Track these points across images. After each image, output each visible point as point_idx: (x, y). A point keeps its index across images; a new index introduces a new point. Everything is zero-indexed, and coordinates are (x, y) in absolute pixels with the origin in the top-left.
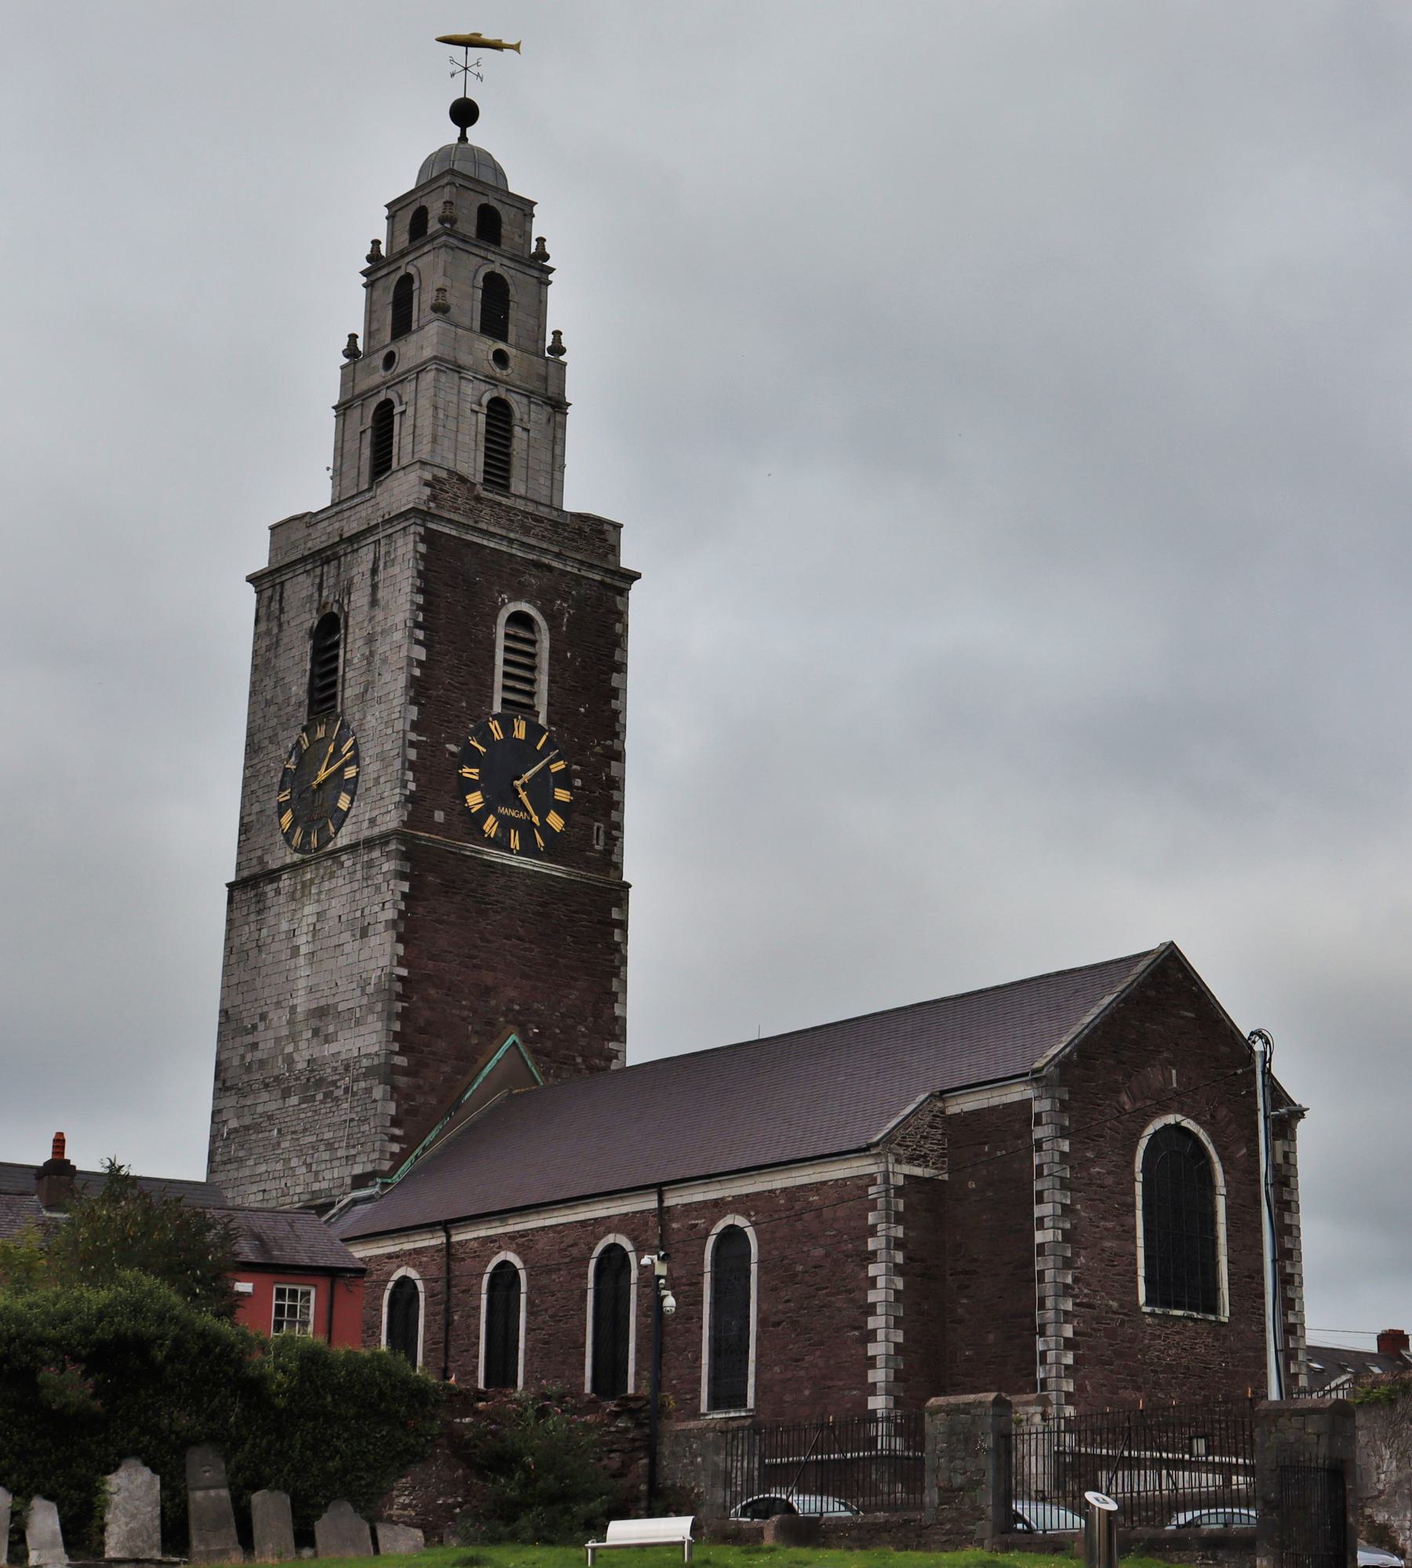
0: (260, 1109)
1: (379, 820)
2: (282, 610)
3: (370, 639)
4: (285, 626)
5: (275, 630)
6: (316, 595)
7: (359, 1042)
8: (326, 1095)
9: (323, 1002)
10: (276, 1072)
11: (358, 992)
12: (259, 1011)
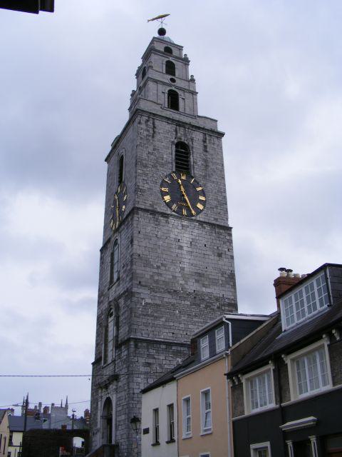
0: (166, 300)
1: (219, 220)
2: (154, 127)
3: (206, 161)
5: (151, 132)
8: (207, 307)
9: (199, 271)
11: (220, 275)
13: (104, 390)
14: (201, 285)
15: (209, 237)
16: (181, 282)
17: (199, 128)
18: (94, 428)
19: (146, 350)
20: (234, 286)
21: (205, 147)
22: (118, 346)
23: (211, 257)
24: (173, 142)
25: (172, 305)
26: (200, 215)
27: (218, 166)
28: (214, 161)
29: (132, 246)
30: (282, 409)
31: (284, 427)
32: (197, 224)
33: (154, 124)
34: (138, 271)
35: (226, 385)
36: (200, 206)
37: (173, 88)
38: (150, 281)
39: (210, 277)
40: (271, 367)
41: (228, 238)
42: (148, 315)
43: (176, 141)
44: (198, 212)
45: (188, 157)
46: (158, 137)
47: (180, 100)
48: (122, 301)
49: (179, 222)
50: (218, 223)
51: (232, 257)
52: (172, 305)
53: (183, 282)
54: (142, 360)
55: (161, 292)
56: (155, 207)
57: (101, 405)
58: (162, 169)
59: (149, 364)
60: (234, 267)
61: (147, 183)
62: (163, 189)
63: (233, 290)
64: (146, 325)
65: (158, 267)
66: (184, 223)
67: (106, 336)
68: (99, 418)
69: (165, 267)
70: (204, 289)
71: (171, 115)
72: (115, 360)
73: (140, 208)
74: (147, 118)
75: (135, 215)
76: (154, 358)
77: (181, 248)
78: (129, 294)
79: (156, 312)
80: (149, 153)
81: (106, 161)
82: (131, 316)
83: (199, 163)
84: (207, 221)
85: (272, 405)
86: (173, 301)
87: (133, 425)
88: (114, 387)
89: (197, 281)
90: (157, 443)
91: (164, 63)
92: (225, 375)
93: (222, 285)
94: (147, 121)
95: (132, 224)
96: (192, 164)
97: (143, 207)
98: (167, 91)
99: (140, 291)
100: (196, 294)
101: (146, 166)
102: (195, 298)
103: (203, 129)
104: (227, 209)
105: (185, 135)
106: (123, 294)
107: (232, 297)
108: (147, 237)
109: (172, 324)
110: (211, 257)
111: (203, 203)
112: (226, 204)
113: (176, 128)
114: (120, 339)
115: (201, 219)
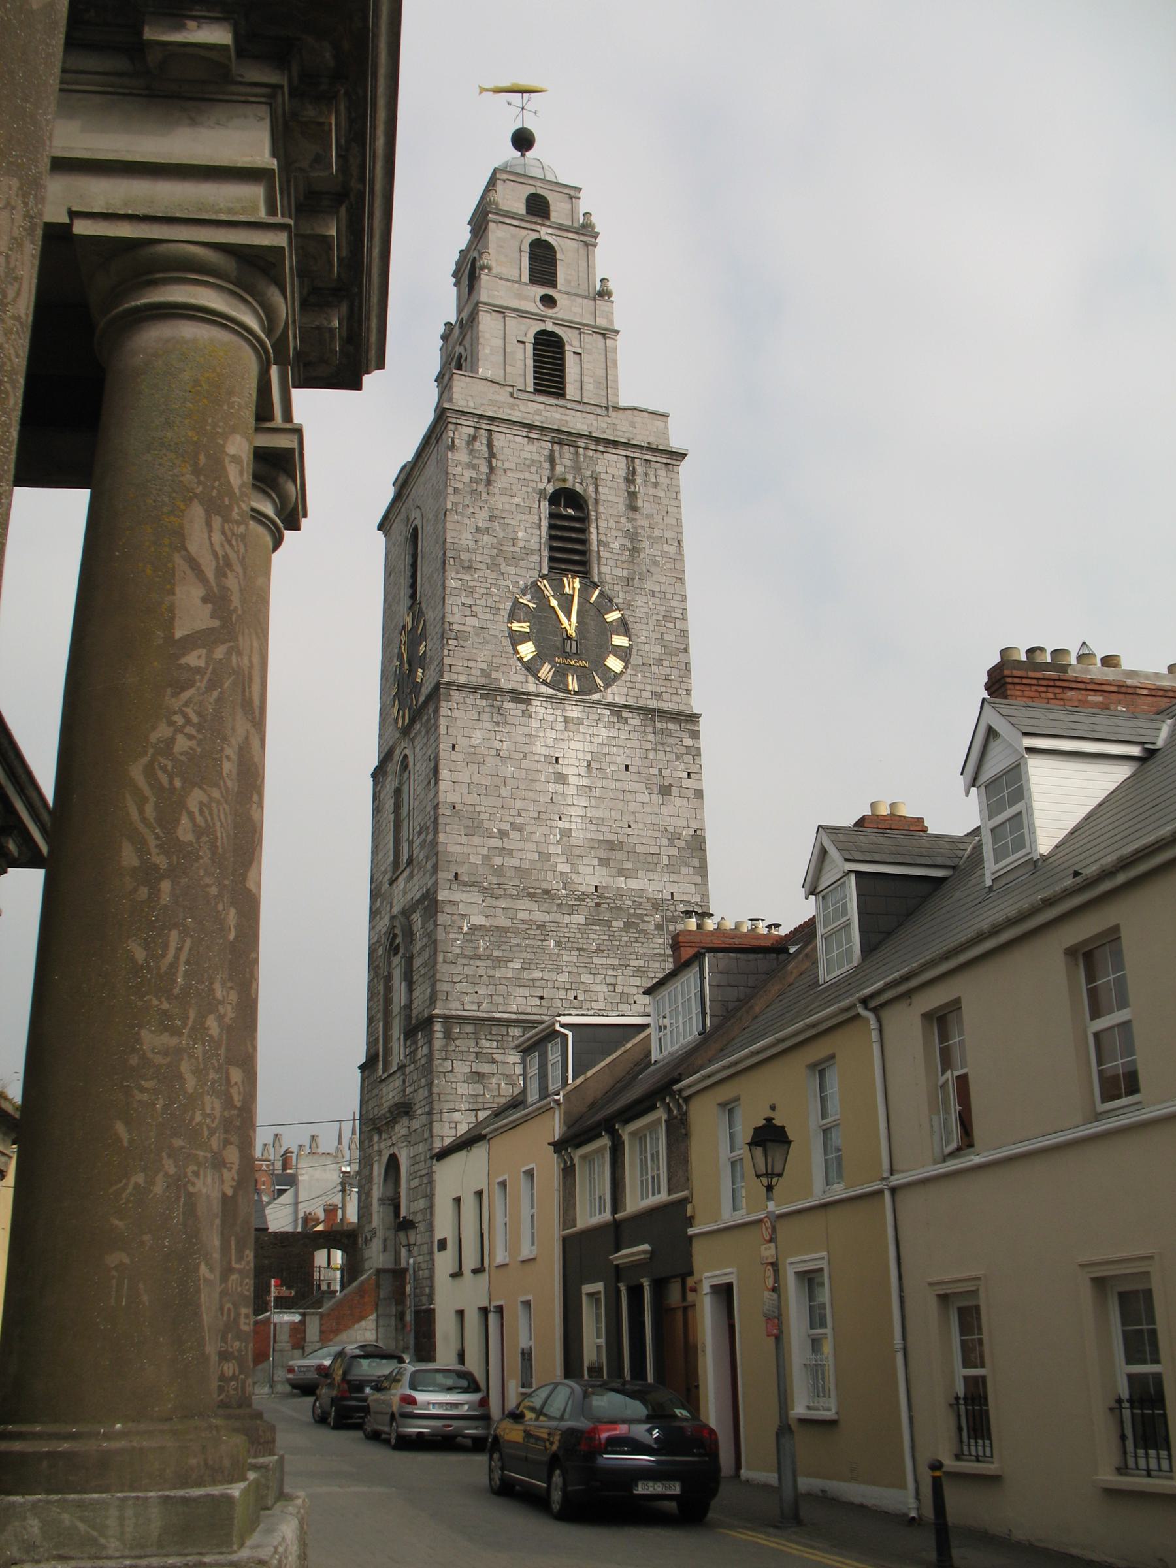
0: (522, 915)
2: (492, 455)
3: (632, 536)
5: (484, 469)
6: (547, 465)
8: (628, 926)
10: (544, 886)
11: (664, 842)
13: (384, 1136)
14: (615, 872)
15: (637, 744)
16: (560, 867)
17: (615, 444)
18: (367, 1229)
19: (472, 1043)
20: (702, 870)
21: (632, 496)
22: (410, 1033)
23: (640, 797)
24: (542, 492)
25: (539, 927)
27: (666, 548)
28: (657, 533)
29: (437, 782)
30: (617, 1225)
31: (617, 1258)
32: (607, 712)
33: (490, 445)
34: (450, 849)
35: (549, 1165)
36: (614, 664)
37: (550, 327)
38: (481, 871)
40: (605, 1141)
41: (688, 742)
42: (479, 957)
43: (550, 489)
44: (611, 678)
45: (584, 531)
46: (500, 482)
47: (570, 361)
48: (417, 918)
49: (559, 712)
50: (662, 705)
51: (699, 794)
52: (539, 927)
53: (567, 868)
54: (462, 1068)
55: (511, 896)
57: (378, 1171)
58: (512, 570)
59: (479, 1077)
60: (702, 820)
62: (515, 626)
63: (699, 880)
64: (473, 981)
65: (503, 834)
66: (569, 714)
67: (388, 1001)
68: (375, 1202)
69: (521, 830)
70: (621, 882)
71: (538, 412)
72: (405, 1066)
73: (453, 684)
74: (471, 431)
75: (443, 704)
76: (494, 1062)
77: (562, 778)
78: (429, 904)
80: (478, 529)
81: (380, 528)
82: (435, 963)
83: (615, 545)
84: (631, 702)
85: (607, 1216)
87: (402, 1235)
88: (404, 1131)
89: (603, 862)
90: (457, 1275)
91: (526, 247)
92: (550, 1144)
93: (669, 869)
94: (474, 438)
95: (437, 727)
96: (594, 547)
97: (462, 679)
98: (530, 338)
99: (456, 897)
100: (602, 897)
101: (470, 568)
102: (598, 905)
103: (627, 445)
105: (577, 469)
107: (698, 899)
108: (474, 758)
110: (640, 797)
111: (624, 654)
112: (686, 650)
113: (552, 451)
114: (414, 1013)
115: (619, 700)
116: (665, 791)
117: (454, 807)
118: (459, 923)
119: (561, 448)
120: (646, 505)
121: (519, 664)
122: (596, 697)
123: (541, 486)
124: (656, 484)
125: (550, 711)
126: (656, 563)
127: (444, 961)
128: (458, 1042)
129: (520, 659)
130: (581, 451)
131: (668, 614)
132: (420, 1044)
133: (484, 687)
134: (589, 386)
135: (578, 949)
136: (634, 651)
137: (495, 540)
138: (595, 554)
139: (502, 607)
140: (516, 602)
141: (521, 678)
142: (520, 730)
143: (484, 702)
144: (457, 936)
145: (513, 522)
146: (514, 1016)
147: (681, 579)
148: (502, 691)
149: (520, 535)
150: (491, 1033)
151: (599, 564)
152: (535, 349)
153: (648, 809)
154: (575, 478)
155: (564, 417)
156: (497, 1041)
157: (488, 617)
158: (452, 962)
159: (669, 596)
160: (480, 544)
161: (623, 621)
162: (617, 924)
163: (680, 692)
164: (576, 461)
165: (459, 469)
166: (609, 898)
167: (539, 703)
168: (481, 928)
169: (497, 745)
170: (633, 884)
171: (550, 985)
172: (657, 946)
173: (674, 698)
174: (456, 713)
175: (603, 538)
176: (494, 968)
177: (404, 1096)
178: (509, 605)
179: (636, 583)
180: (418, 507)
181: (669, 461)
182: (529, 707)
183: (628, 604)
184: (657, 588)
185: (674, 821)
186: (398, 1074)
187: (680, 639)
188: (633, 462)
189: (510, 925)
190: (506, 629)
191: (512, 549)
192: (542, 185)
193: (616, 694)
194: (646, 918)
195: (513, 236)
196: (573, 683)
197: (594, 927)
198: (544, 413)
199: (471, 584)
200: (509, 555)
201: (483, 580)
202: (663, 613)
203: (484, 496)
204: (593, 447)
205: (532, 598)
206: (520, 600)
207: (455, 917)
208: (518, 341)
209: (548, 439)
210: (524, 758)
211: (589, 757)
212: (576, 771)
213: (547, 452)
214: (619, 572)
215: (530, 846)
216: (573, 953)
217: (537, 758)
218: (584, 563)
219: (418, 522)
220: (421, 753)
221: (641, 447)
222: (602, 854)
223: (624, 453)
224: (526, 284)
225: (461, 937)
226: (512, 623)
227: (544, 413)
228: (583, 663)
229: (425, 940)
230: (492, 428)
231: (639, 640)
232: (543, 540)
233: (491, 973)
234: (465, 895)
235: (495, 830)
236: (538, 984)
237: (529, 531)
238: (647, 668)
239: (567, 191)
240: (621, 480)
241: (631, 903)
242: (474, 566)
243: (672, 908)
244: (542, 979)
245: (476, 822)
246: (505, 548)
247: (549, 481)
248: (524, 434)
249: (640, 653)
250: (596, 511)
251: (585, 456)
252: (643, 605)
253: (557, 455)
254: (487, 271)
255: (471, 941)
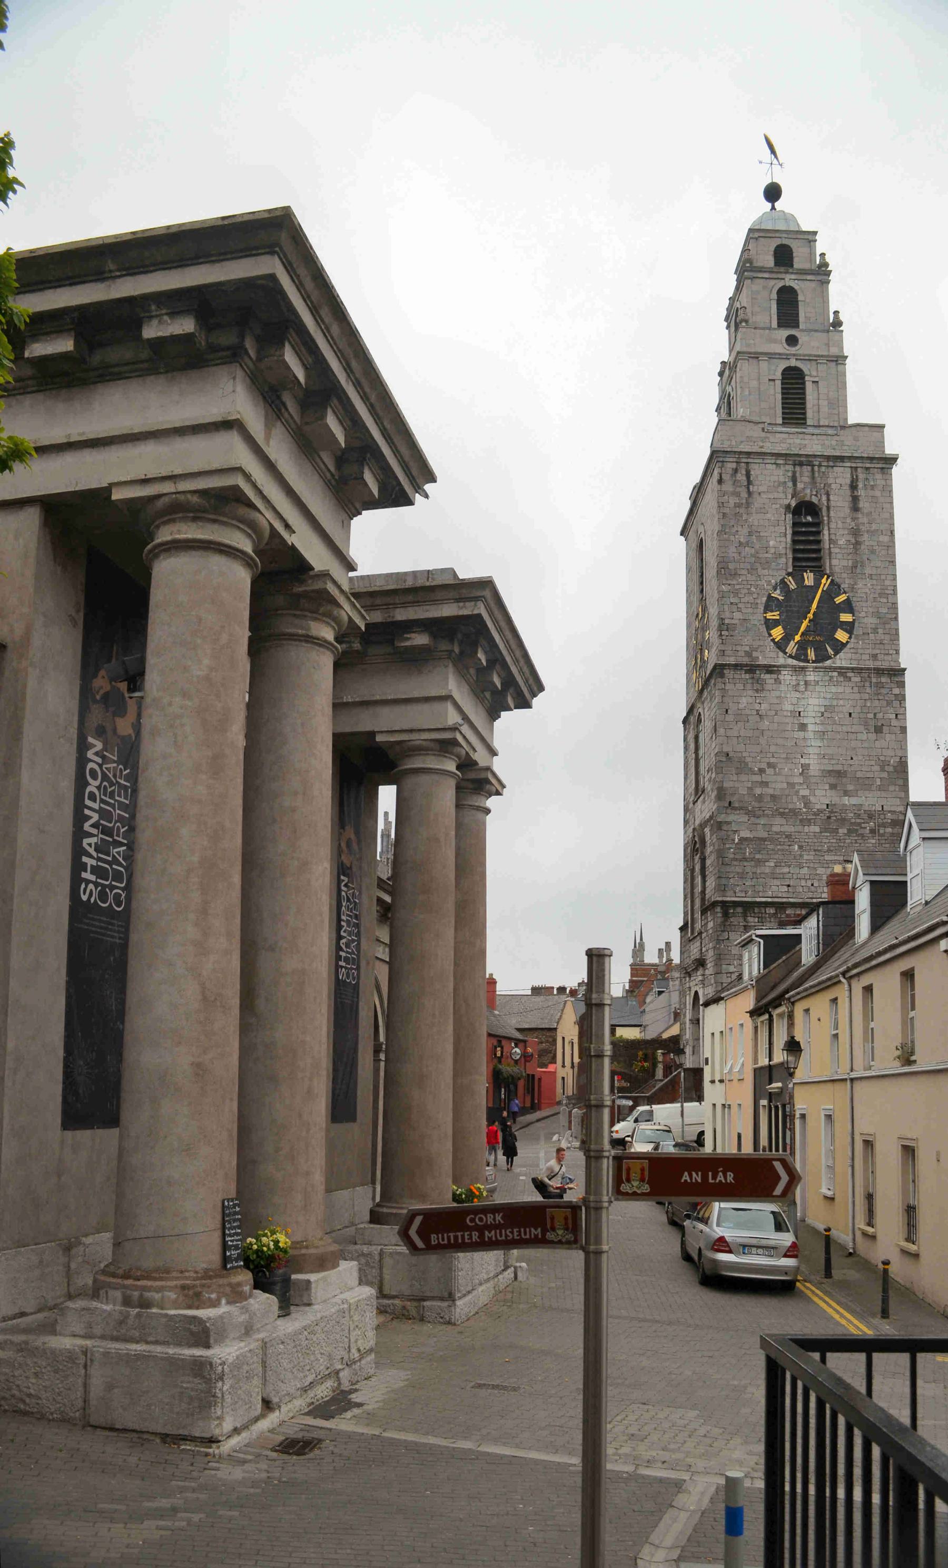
0: (775, 829)
1: (879, 657)
2: (749, 482)
3: (856, 532)
4: (755, 496)
5: (744, 495)
6: (790, 484)
7: (884, 802)
9: (839, 768)
10: (791, 806)
11: (877, 768)
12: (767, 760)
14: (842, 792)
15: (857, 696)
16: (802, 793)
17: (842, 459)
19: (741, 920)
21: (855, 499)
24: (788, 507)
25: (787, 837)
26: (841, 655)
27: (881, 538)
28: (874, 527)
32: (835, 674)
33: (748, 475)
36: (841, 636)
39: (859, 775)
41: (896, 691)
42: (745, 859)
43: (793, 504)
45: (818, 533)
46: (757, 502)
47: (809, 387)
49: (801, 678)
50: (878, 664)
51: (904, 730)
52: (787, 837)
53: (805, 792)
55: (767, 816)
56: (755, 654)
60: (906, 750)
61: (739, 610)
62: (769, 615)
63: (902, 795)
64: (742, 876)
65: (761, 771)
66: (808, 678)
70: (846, 800)
73: (726, 665)
74: (734, 466)
77: (803, 727)
79: (759, 852)
80: (740, 543)
83: (842, 542)
86: (789, 829)
89: (833, 787)
93: (880, 788)
94: (736, 471)
96: (826, 545)
97: (732, 660)
98: (778, 375)
99: (731, 818)
102: (829, 818)
104: (897, 630)
106: (709, 820)
109: (786, 870)
110: (860, 736)
111: (849, 628)
112: (896, 619)
113: (794, 473)
114: (707, 897)
115: (844, 664)
116: (878, 730)
117: (728, 755)
118: (732, 837)
119: (801, 468)
120: (867, 505)
121: (772, 644)
122: (828, 663)
123: (786, 502)
124: (873, 488)
125: (794, 678)
126: (873, 552)
127: (723, 864)
128: (732, 920)
129: (773, 640)
130: (816, 468)
131: (883, 591)
132: (709, 920)
133: (747, 665)
134: (825, 409)
135: (815, 850)
136: (856, 625)
137: (753, 551)
138: (827, 551)
139: (759, 602)
140: (769, 597)
141: (773, 655)
142: (775, 694)
143: (747, 676)
144: (731, 846)
145: (765, 534)
146: (769, 900)
147: (892, 562)
148: (759, 666)
149: (772, 543)
150: (754, 912)
151: (830, 559)
152: (782, 384)
153: (866, 745)
154: (811, 490)
155: (803, 442)
156: (758, 918)
157: (750, 610)
158: (727, 864)
159: (883, 577)
160: (743, 555)
161: (848, 602)
162: (843, 831)
163: (891, 652)
164: (813, 477)
165: (726, 497)
166: (836, 812)
167: (786, 673)
168: (746, 839)
169: (757, 707)
170: (854, 801)
171: (795, 876)
172: (871, 845)
173: (886, 658)
174: (728, 687)
175: (833, 537)
176: (756, 866)
177: (701, 953)
178: (765, 599)
179: (858, 571)
180: (702, 524)
181: (884, 466)
182: (780, 676)
183: (852, 588)
184: (874, 572)
185: (885, 752)
186: (698, 938)
187: (891, 611)
188: (856, 471)
189: (767, 836)
190: (762, 618)
191: (767, 555)
192: (786, 236)
193: (842, 660)
194: (863, 825)
195: (764, 288)
196: (811, 654)
197: (826, 834)
198: (788, 441)
199: (737, 587)
200: (763, 561)
201: (745, 583)
202: (879, 591)
203: (745, 517)
204: (825, 464)
205: (781, 592)
206: (773, 595)
207: (730, 833)
208: (769, 380)
209: (791, 463)
210: (776, 714)
211: (823, 710)
212: (813, 721)
213: (790, 474)
214: (845, 563)
215: (779, 778)
216: (811, 853)
217: (785, 713)
218: (819, 559)
219: (702, 535)
220: (708, 714)
221: (862, 458)
222: (832, 780)
223: (848, 464)
224: (775, 329)
225: (734, 846)
226: (766, 613)
227: (788, 441)
228: (818, 638)
229: (712, 847)
230: (749, 460)
231: (860, 615)
232: (788, 546)
233: (754, 870)
234: (736, 817)
235: (756, 769)
236: (787, 876)
237: (778, 539)
238: (866, 637)
239: (806, 237)
240: (847, 487)
241: (852, 815)
242: (739, 573)
243: (882, 817)
244: (789, 873)
245: (743, 764)
246: (761, 556)
247: (792, 498)
248: (773, 461)
249: (862, 625)
250: (828, 516)
251: (819, 471)
252: (864, 587)
253: (798, 475)
254: (744, 324)
255: (741, 849)
